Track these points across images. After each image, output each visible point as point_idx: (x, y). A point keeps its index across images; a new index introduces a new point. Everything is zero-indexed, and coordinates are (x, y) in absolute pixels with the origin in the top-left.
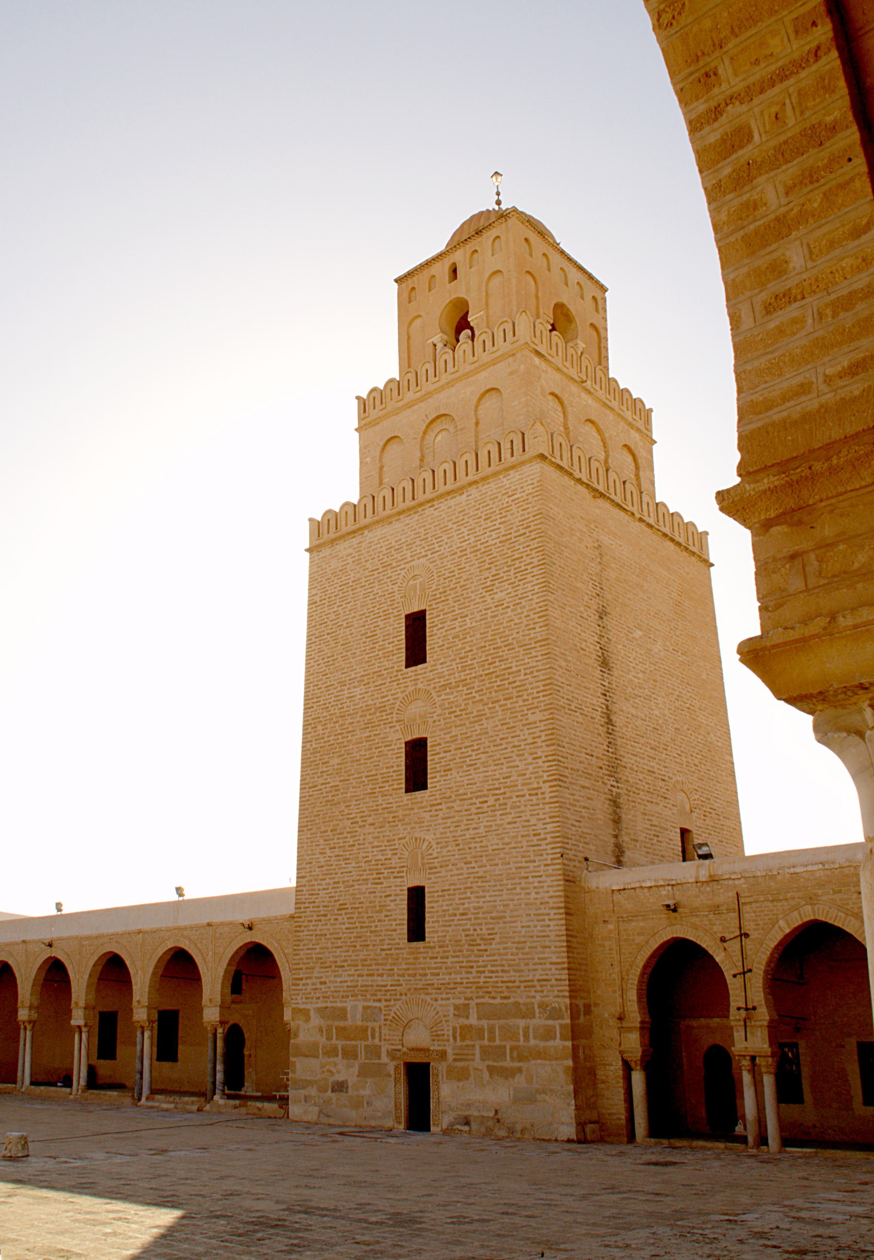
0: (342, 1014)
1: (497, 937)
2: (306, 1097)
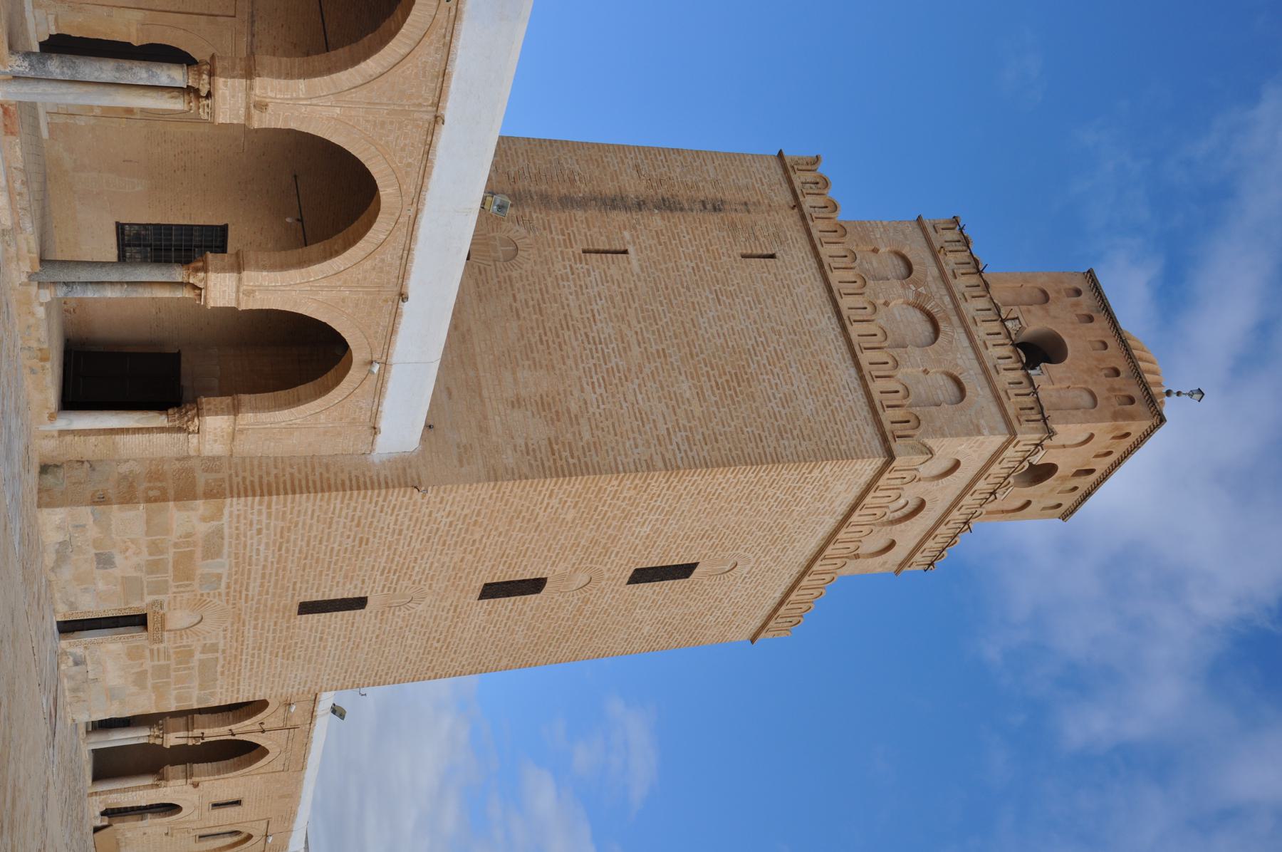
1: (290, 661)
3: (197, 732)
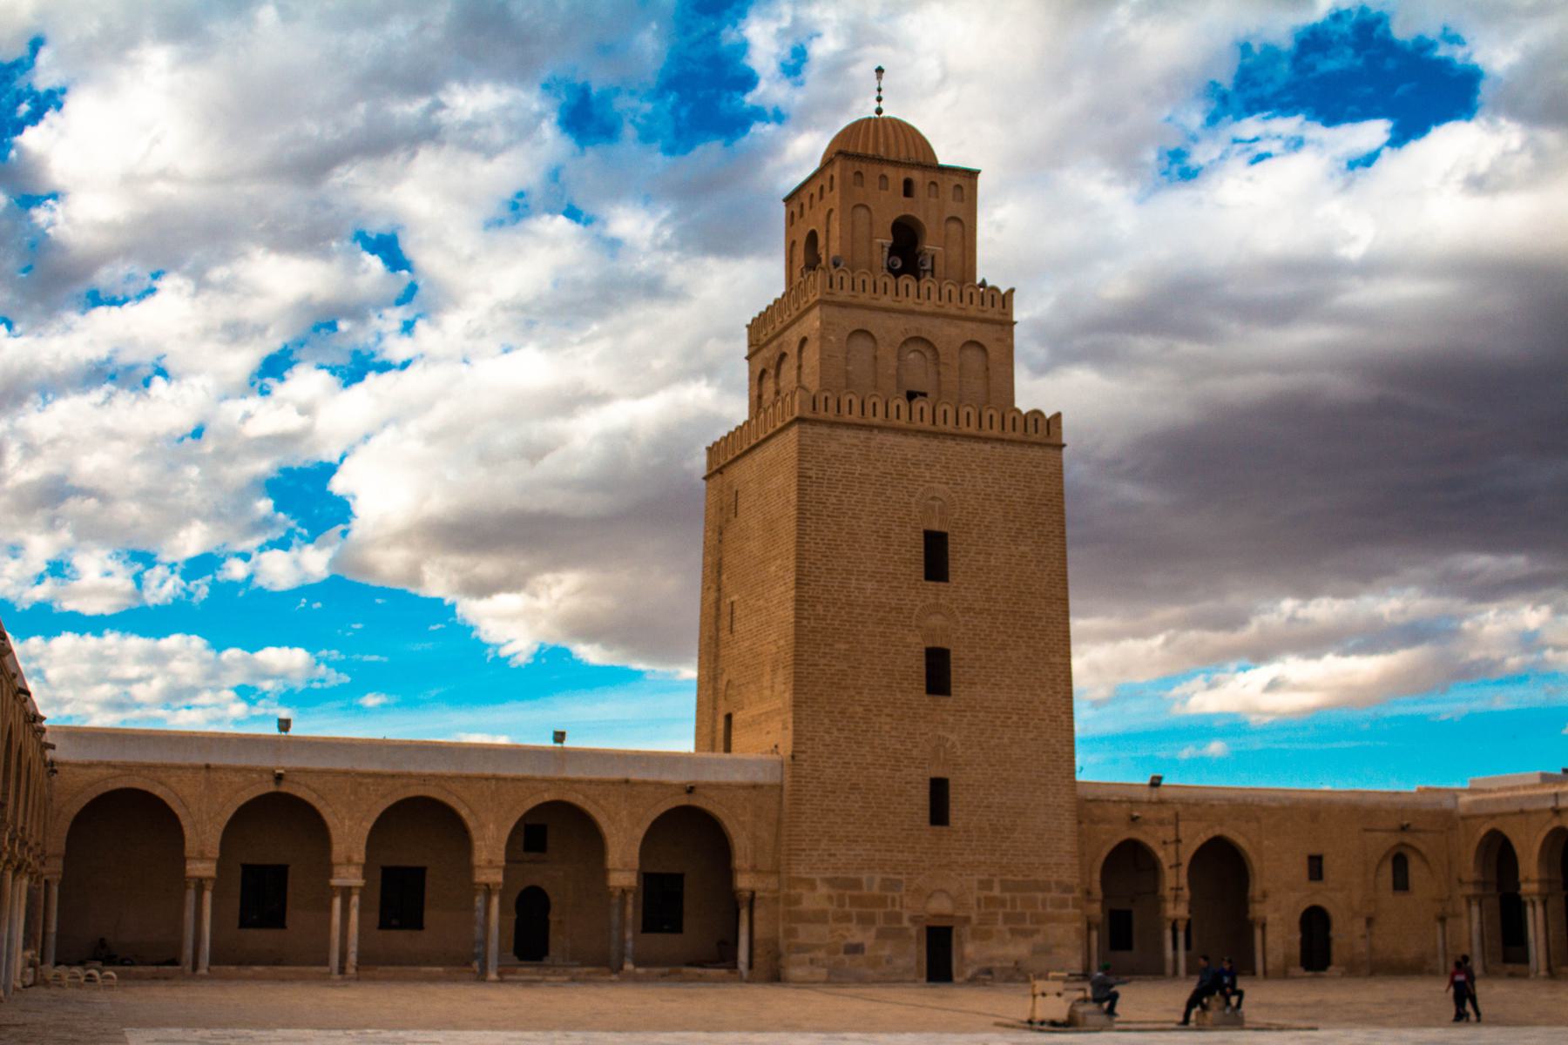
0: (857, 884)
2: (812, 961)
3: (1168, 893)
